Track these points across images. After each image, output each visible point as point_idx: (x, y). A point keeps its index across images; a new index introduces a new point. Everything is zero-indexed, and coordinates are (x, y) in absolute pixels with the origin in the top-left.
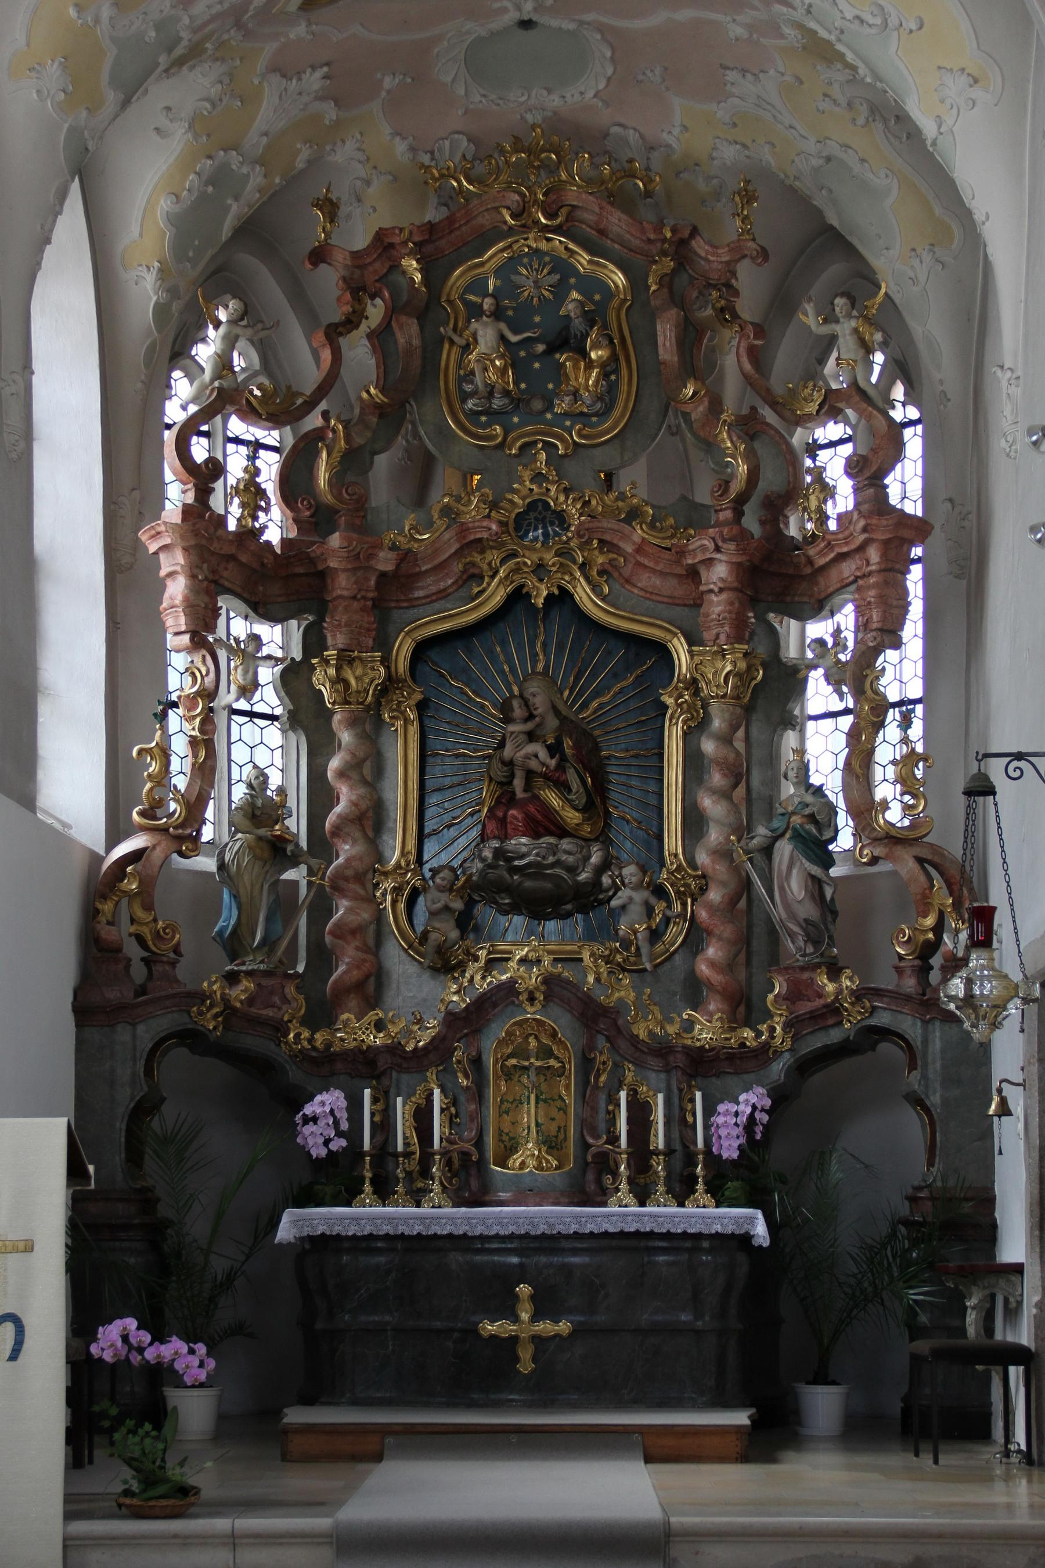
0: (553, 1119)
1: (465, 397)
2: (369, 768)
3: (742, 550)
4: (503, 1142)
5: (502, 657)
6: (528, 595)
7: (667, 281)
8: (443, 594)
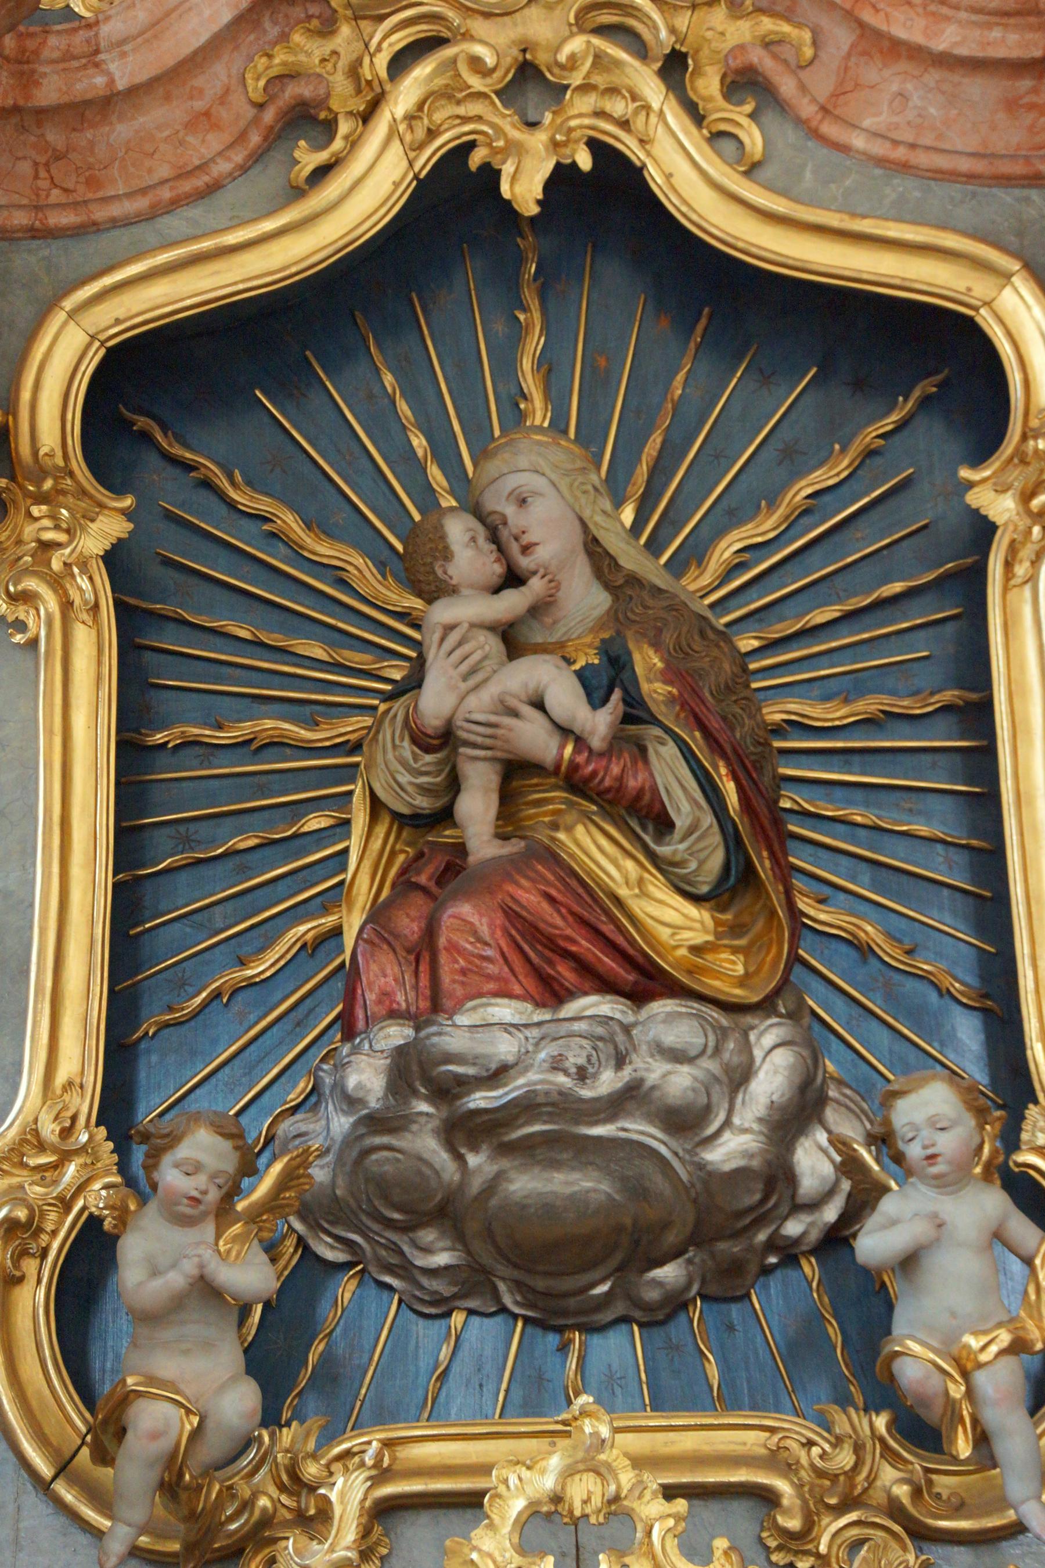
5: (403, 407)
6: (490, 175)
8: (200, 181)
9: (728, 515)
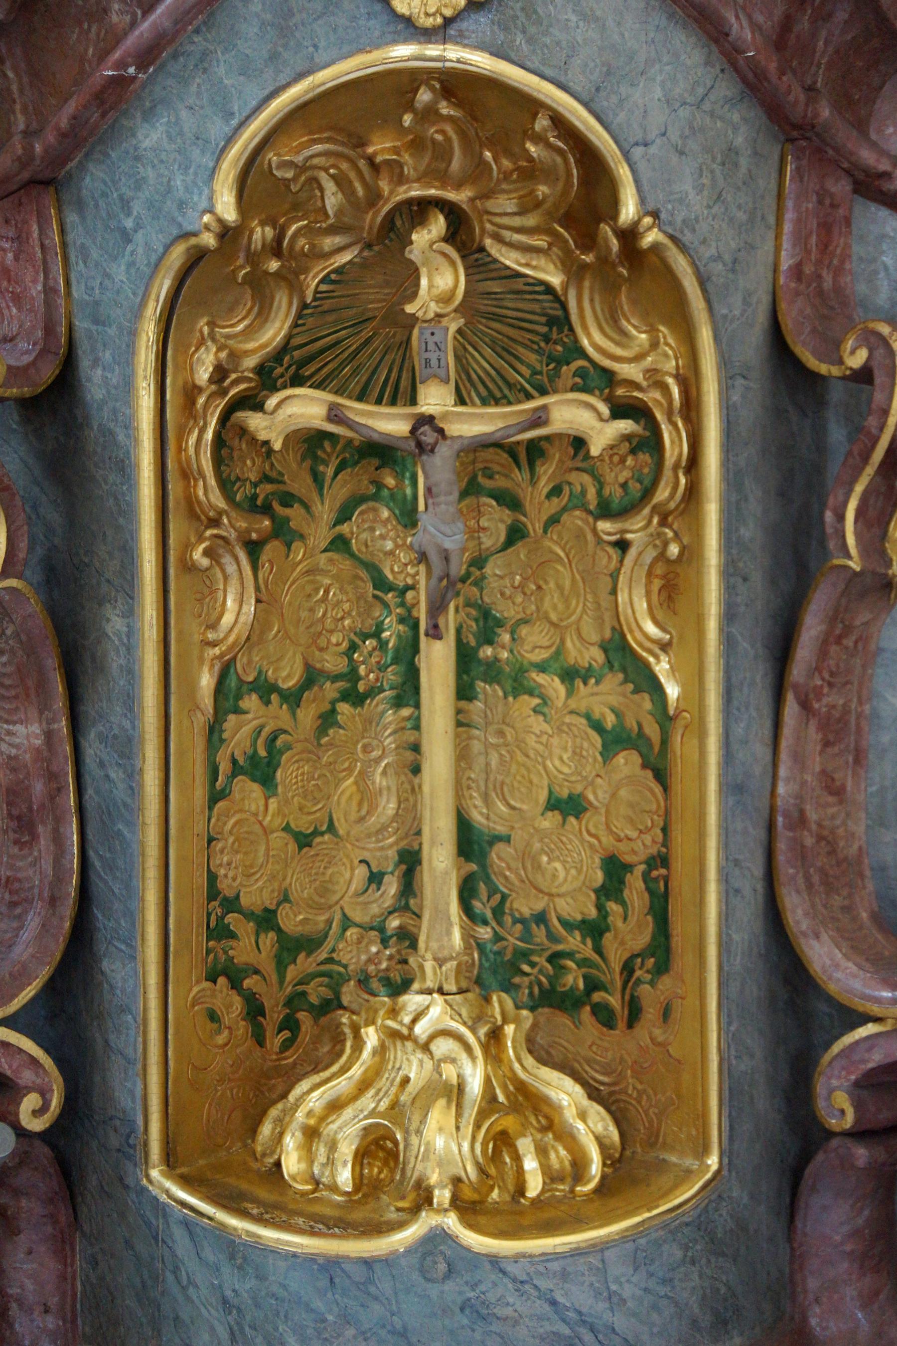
0: (568, 806)
4: (231, 974)
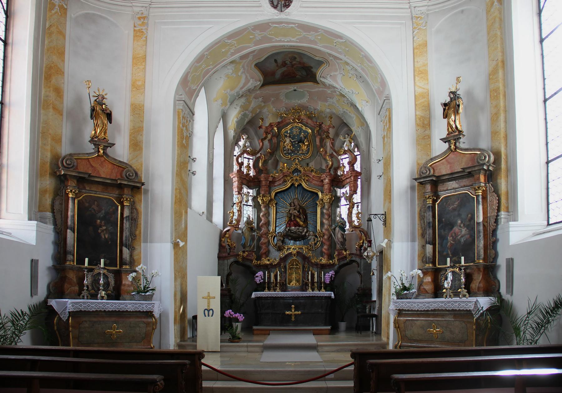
1: (284, 151)
2: (267, 214)
3: (330, 177)
7: (318, 131)
9: (306, 202)
